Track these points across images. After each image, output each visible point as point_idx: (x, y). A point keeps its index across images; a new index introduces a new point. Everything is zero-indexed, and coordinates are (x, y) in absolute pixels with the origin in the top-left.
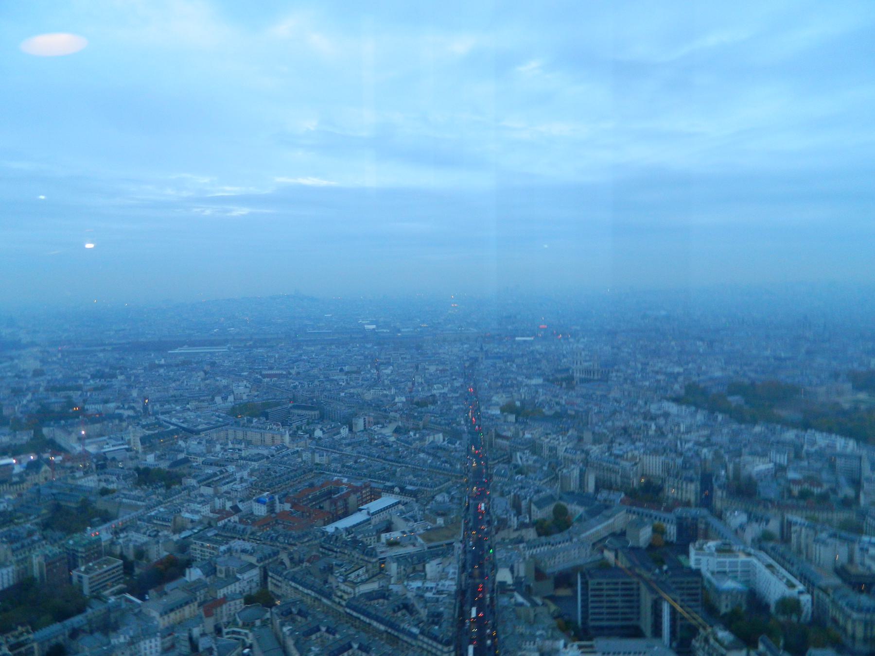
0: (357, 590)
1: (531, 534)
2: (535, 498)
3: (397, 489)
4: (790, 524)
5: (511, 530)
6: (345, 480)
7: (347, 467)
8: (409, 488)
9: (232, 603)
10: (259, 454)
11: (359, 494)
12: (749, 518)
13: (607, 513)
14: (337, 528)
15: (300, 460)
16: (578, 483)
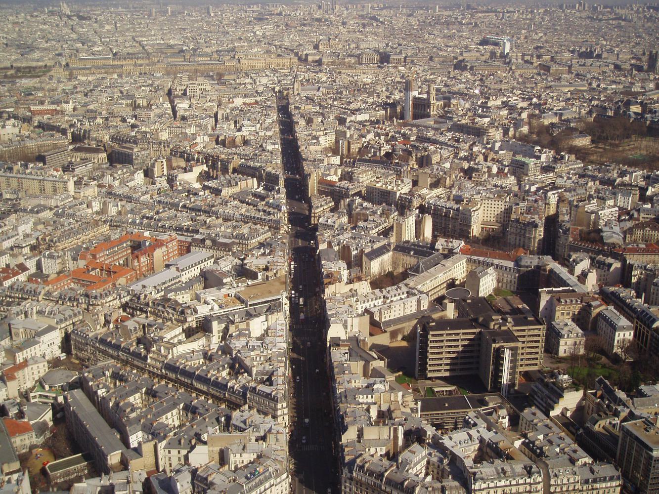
0: (175, 349)
1: (364, 287)
2: (367, 250)
3: (208, 242)
4: (631, 267)
5: (343, 283)
6: (147, 234)
7: (147, 218)
8: (222, 240)
9: (35, 366)
10: (39, 205)
11: (164, 248)
12: (592, 265)
13: (444, 262)
14: (144, 287)
15: (90, 211)
16: (414, 232)
